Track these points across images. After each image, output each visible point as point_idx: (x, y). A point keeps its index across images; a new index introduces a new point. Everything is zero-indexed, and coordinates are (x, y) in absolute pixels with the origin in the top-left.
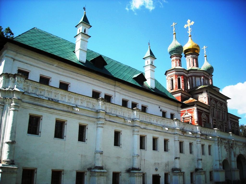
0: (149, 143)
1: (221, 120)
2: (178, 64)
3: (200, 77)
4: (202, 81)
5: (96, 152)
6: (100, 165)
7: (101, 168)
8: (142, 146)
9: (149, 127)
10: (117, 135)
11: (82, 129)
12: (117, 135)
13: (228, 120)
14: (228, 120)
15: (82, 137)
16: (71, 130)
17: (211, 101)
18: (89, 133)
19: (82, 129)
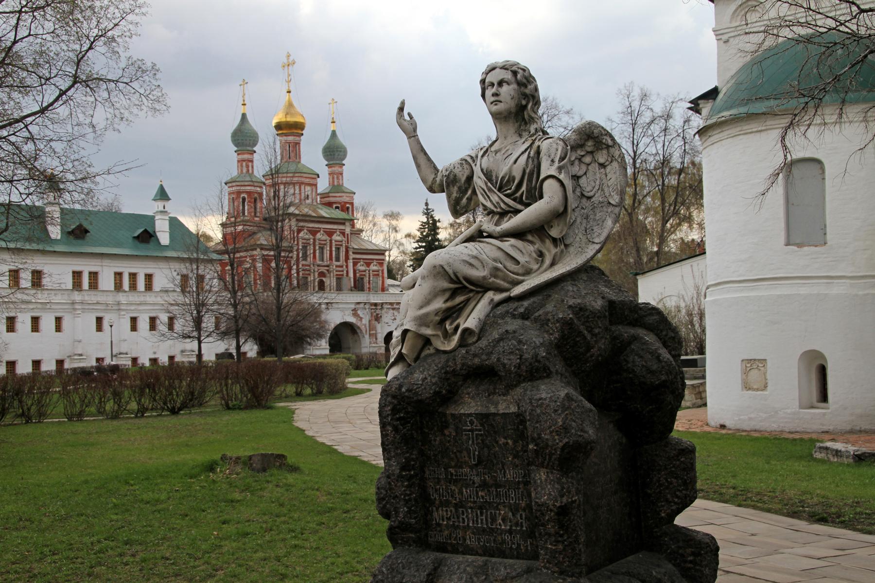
0: (143, 324)
1: (325, 263)
2: (245, 170)
3: (294, 184)
4: (297, 191)
5: (75, 341)
6: (80, 353)
7: (81, 355)
8: (134, 328)
9: (141, 308)
10: (99, 320)
11: (58, 320)
12: (99, 320)
13: (347, 258)
14: (347, 258)
15: (58, 328)
16: (47, 323)
17: (298, 234)
18: (65, 324)
19: (58, 320)
